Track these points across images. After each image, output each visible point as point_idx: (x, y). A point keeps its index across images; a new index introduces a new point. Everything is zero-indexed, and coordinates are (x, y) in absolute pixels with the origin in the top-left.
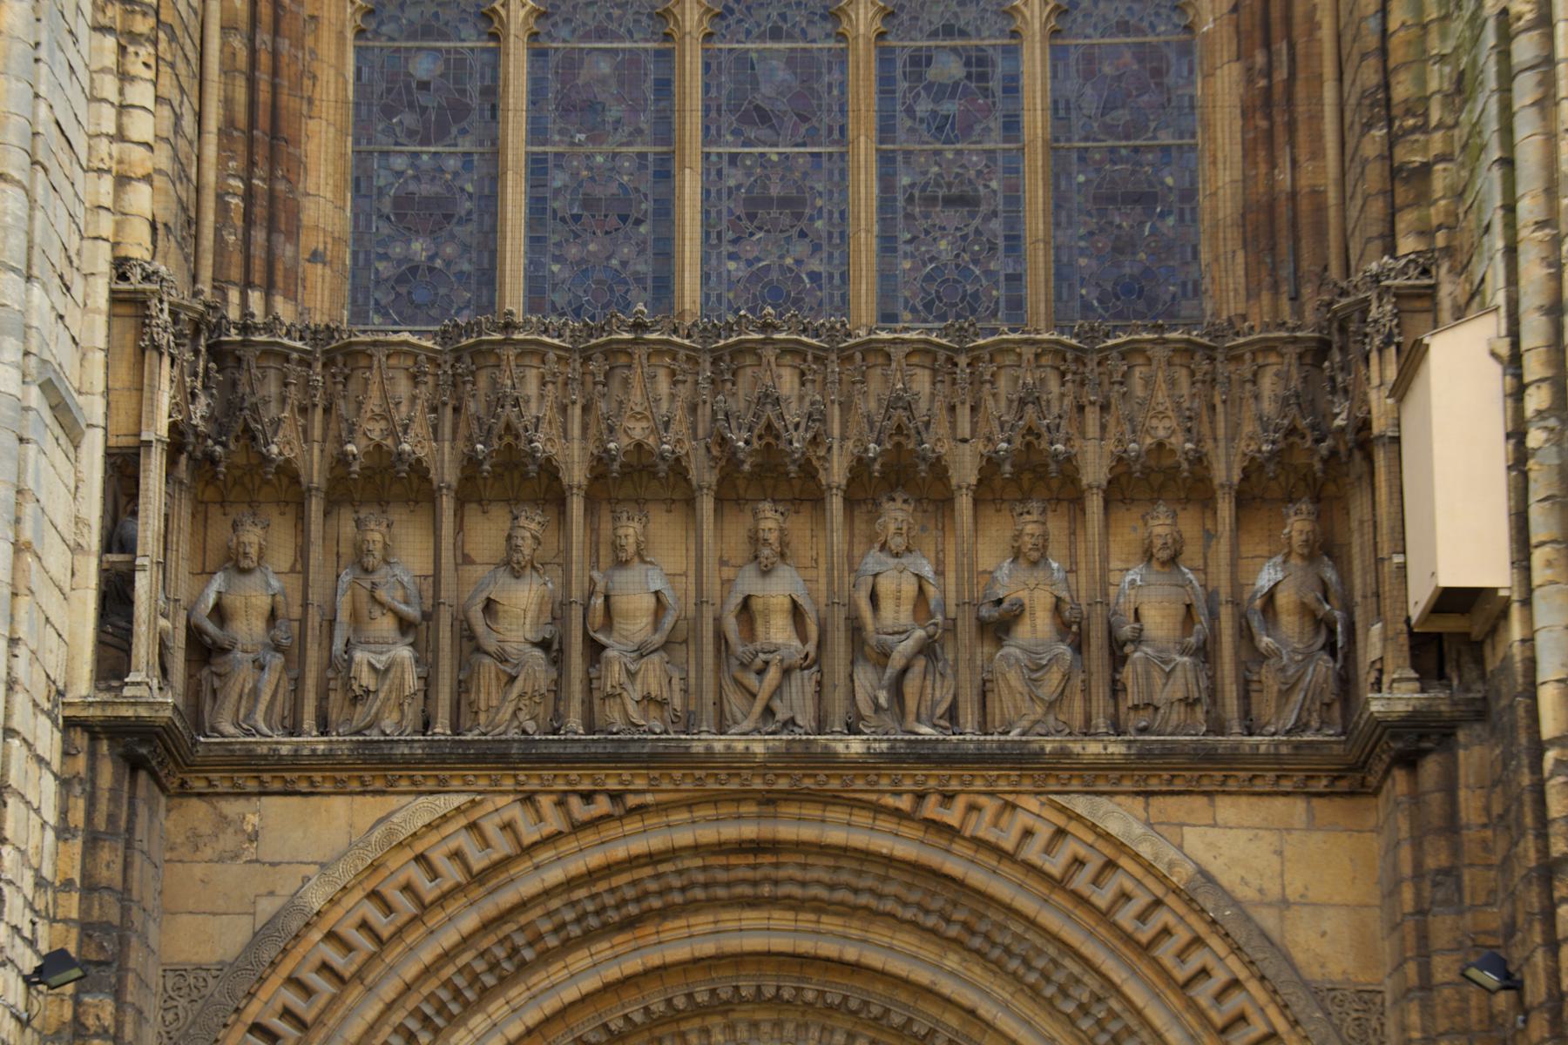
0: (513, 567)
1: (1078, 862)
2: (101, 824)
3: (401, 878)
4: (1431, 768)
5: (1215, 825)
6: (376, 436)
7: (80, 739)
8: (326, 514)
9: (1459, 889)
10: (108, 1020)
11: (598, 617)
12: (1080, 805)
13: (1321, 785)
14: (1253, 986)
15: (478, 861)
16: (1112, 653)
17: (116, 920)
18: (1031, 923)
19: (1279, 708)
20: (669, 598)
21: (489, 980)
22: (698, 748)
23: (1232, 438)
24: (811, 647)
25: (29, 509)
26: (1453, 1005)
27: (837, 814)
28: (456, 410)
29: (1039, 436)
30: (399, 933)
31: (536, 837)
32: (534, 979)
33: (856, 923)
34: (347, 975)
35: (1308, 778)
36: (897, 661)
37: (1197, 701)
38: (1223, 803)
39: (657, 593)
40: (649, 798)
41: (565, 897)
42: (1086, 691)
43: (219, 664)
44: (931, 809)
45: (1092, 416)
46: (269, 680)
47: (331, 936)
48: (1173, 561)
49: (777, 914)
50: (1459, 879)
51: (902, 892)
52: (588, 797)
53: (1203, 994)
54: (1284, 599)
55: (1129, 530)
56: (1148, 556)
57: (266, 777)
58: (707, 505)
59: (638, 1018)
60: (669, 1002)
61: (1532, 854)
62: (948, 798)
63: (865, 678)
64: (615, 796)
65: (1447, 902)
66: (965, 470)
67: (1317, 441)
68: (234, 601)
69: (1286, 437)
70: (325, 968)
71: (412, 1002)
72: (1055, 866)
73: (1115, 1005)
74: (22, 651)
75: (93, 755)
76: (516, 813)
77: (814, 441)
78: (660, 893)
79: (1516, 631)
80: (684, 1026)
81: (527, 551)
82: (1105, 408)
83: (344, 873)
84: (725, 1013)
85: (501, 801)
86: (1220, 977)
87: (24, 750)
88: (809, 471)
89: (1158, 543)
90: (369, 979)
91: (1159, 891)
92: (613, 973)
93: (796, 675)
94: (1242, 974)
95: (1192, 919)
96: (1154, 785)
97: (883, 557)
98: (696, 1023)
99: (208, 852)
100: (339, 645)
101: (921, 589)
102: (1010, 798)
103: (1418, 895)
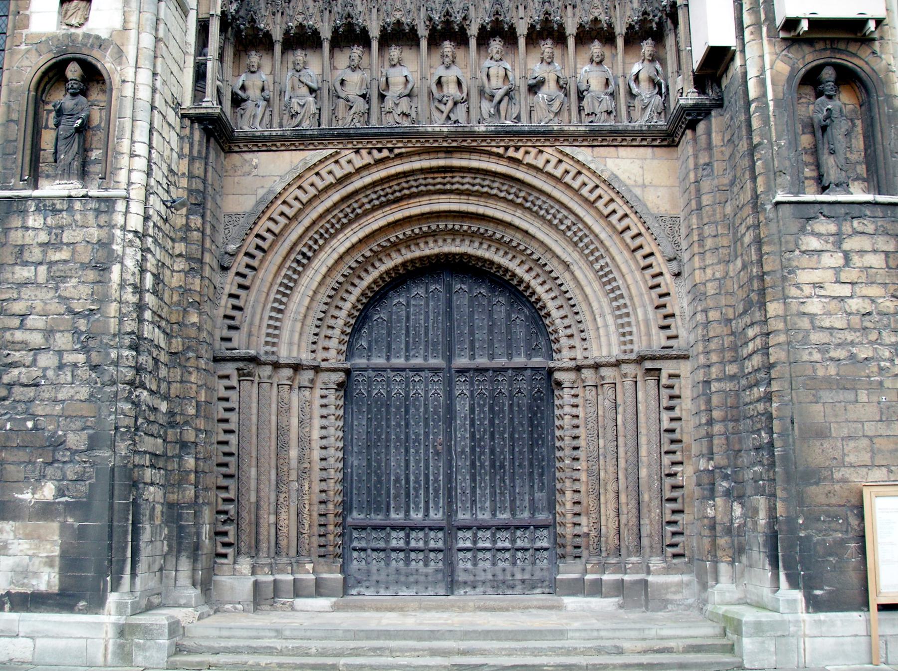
0: (354, 68)
1: (567, 172)
2: (195, 154)
3: (310, 181)
4: (701, 127)
5: (618, 158)
6: (300, 20)
7: (187, 122)
8: (283, 53)
9: (712, 171)
10: (199, 225)
11: (383, 85)
12: (568, 150)
13: (657, 143)
14: (632, 216)
15: (339, 174)
16: (579, 97)
17: (202, 189)
18: (549, 196)
19: (642, 115)
20: (410, 78)
21: (345, 221)
22: (422, 130)
23: (621, 18)
24: (465, 95)
25: (161, 26)
26: (710, 213)
27: (475, 156)
28: (330, 12)
29: (550, 15)
30: (310, 201)
31: (361, 165)
32: (362, 221)
33: (483, 200)
34: (291, 216)
35: (653, 140)
36: (497, 98)
37: (611, 112)
38: (621, 149)
39: (406, 76)
40: (403, 150)
41: (372, 190)
42: (569, 110)
43: (243, 105)
44: (511, 153)
45: (569, 8)
46: (260, 111)
47: (284, 202)
48: (600, 63)
49: (452, 196)
50: (712, 166)
51: (500, 186)
52: (380, 150)
53: (614, 219)
54: (642, 76)
55: (585, 55)
56: (592, 61)
57: (260, 144)
58: (424, 43)
59: (401, 237)
60: (413, 231)
61: (745, 145)
62: (517, 149)
63: (487, 107)
64: (391, 150)
65: (708, 175)
66: (522, 29)
67: (654, 16)
68: (248, 84)
69: (643, 15)
70: (282, 214)
71: (316, 228)
72: (558, 173)
73: (581, 227)
74: (158, 78)
75: (192, 128)
76: (353, 156)
77: (465, 19)
79: (738, 61)
80: (418, 241)
81: (356, 61)
82: (574, 7)
83: (289, 179)
84: (434, 236)
85: (347, 152)
86: (620, 213)
87: (161, 117)
88: (463, 30)
89: (595, 55)
90: (299, 220)
91: (598, 182)
92: (391, 219)
93: (459, 106)
94: (628, 212)
95: (610, 192)
96: (595, 143)
97: (493, 62)
98: (423, 240)
99: (239, 173)
100: (287, 98)
101: (506, 74)
102: (541, 148)
103: (696, 175)
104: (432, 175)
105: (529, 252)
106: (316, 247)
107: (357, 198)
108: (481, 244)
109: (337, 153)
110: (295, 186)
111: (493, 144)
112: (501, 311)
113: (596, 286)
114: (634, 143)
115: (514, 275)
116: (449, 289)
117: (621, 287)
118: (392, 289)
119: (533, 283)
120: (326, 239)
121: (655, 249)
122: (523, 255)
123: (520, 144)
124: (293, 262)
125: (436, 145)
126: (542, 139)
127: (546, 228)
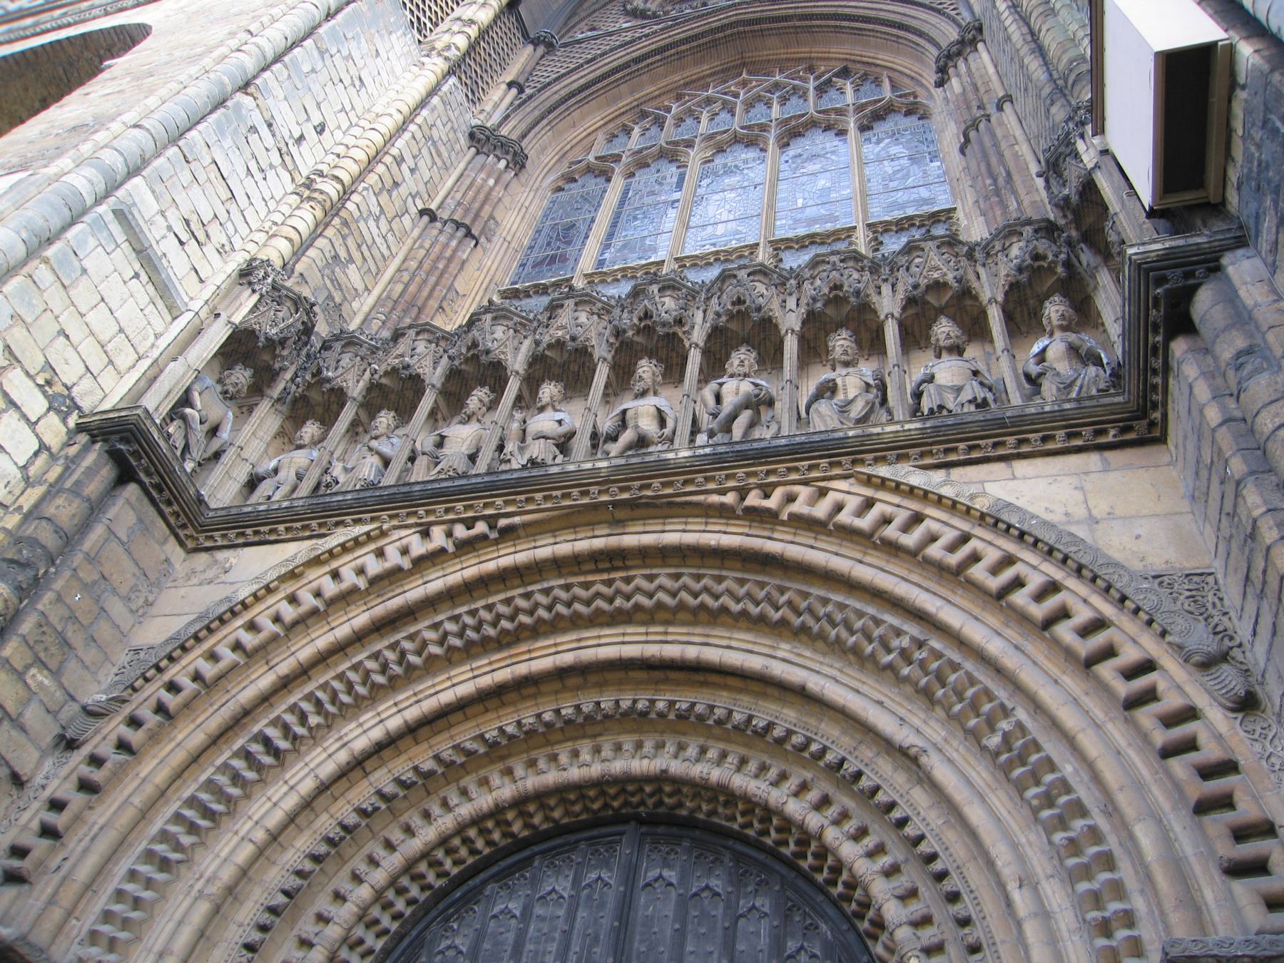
5: (1014, 478)
12: (883, 471)
13: (1110, 438)
21: (380, 679)
40: (517, 520)
44: (753, 499)
52: (469, 523)
64: (491, 521)
78: (531, 613)
85: (404, 533)
96: (953, 457)
104: (582, 579)
105: (814, 747)
106: (300, 730)
107: (412, 629)
108: (703, 751)
109: (383, 534)
110: (281, 595)
111: (711, 486)
112: (758, 934)
113: (1001, 801)
114: (1050, 446)
115: (787, 825)
116: (630, 876)
117: (1072, 781)
118: (496, 877)
119: (831, 834)
120: (327, 715)
121: (1151, 646)
122: (804, 764)
123: (772, 479)
124: (236, 755)
125: (586, 500)
126: (824, 462)
127: (852, 675)
